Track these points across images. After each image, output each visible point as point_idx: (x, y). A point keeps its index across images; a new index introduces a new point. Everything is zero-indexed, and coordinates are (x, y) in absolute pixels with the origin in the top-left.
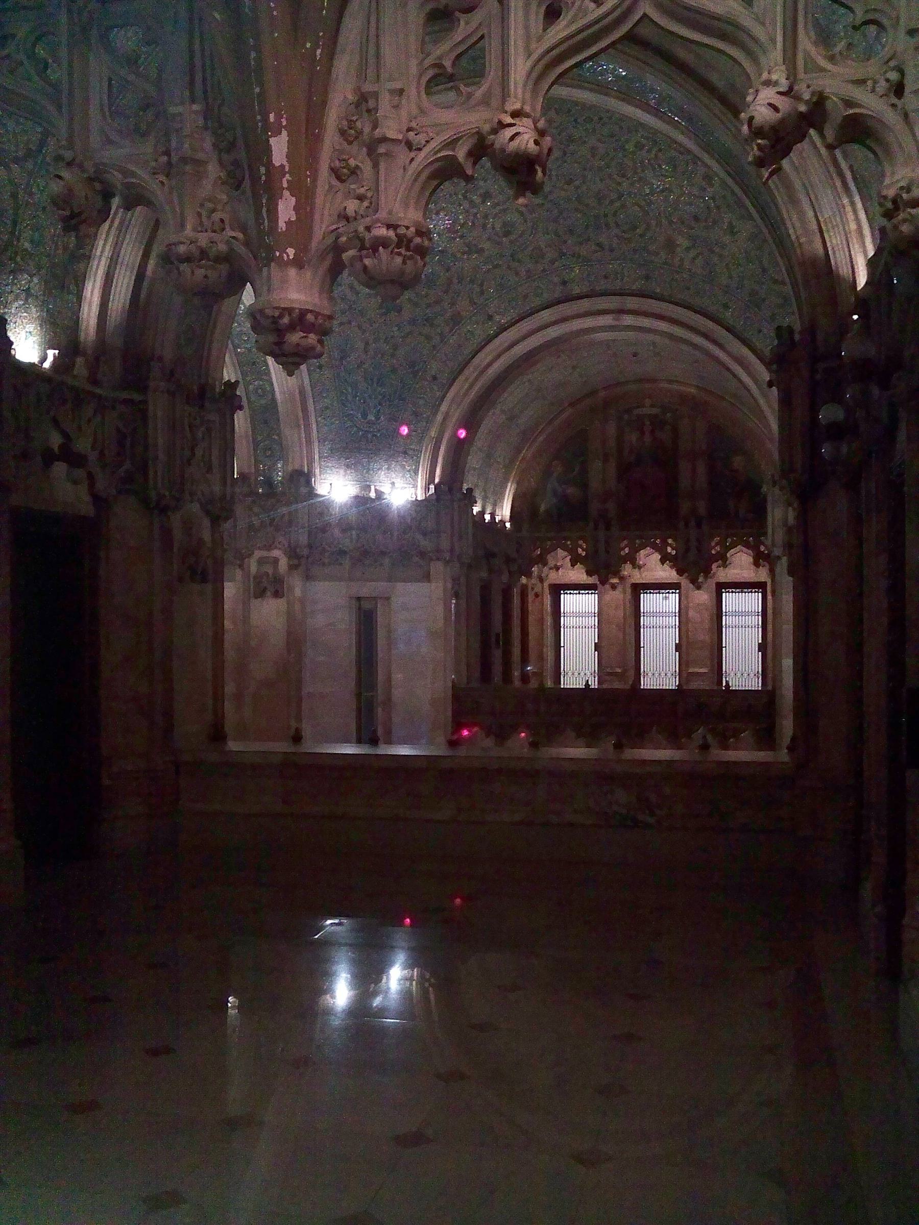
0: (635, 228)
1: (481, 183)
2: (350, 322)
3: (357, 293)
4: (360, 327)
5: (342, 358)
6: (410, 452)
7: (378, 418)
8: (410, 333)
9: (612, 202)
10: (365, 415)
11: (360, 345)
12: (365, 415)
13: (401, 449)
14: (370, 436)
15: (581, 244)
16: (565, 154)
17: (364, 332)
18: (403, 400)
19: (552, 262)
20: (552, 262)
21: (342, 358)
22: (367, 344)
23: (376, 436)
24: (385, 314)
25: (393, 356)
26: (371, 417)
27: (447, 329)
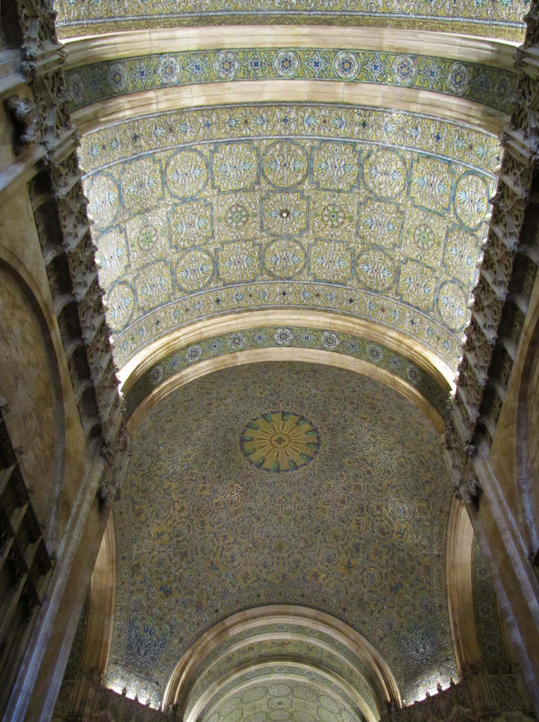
0: (423, 463)
1: (371, 505)
2: (383, 608)
3: (376, 592)
4: (389, 607)
5: (391, 628)
6: (450, 657)
7: (425, 649)
8: (415, 593)
9: (406, 462)
10: (417, 651)
11: (395, 615)
12: (417, 651)
13: (444, 659)
14: (424, 661)
15: (424, 489)
16: (371, 465)
17: (393, 608)
18: (434, 629)
19: (429, 508)
20: (429, 508)
21: (391, 628)
22: (398, 612)
23: (428, 659)
24: (397, 592)
25: (415, 610)
26: (422, 650)
27: (428, 577)
